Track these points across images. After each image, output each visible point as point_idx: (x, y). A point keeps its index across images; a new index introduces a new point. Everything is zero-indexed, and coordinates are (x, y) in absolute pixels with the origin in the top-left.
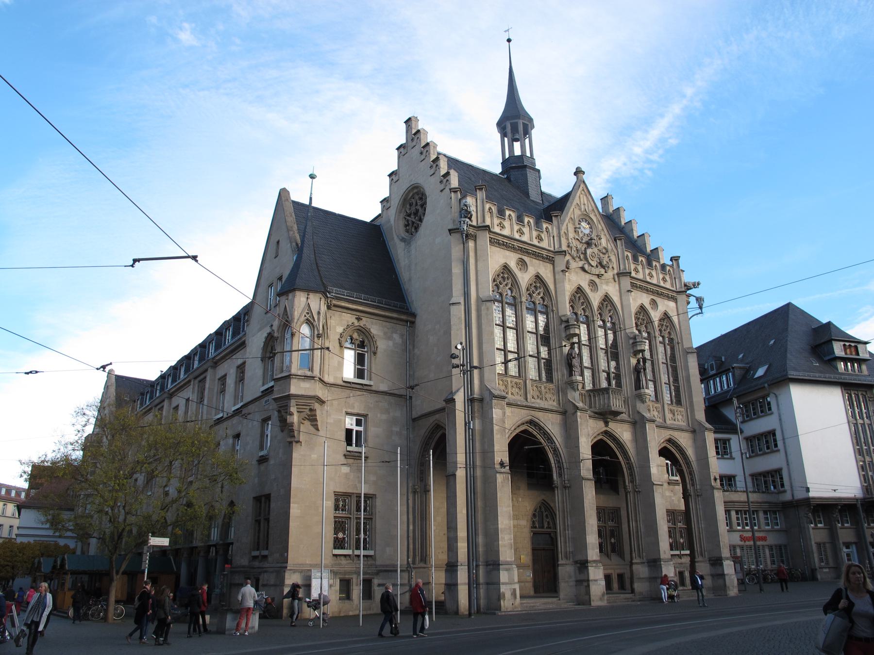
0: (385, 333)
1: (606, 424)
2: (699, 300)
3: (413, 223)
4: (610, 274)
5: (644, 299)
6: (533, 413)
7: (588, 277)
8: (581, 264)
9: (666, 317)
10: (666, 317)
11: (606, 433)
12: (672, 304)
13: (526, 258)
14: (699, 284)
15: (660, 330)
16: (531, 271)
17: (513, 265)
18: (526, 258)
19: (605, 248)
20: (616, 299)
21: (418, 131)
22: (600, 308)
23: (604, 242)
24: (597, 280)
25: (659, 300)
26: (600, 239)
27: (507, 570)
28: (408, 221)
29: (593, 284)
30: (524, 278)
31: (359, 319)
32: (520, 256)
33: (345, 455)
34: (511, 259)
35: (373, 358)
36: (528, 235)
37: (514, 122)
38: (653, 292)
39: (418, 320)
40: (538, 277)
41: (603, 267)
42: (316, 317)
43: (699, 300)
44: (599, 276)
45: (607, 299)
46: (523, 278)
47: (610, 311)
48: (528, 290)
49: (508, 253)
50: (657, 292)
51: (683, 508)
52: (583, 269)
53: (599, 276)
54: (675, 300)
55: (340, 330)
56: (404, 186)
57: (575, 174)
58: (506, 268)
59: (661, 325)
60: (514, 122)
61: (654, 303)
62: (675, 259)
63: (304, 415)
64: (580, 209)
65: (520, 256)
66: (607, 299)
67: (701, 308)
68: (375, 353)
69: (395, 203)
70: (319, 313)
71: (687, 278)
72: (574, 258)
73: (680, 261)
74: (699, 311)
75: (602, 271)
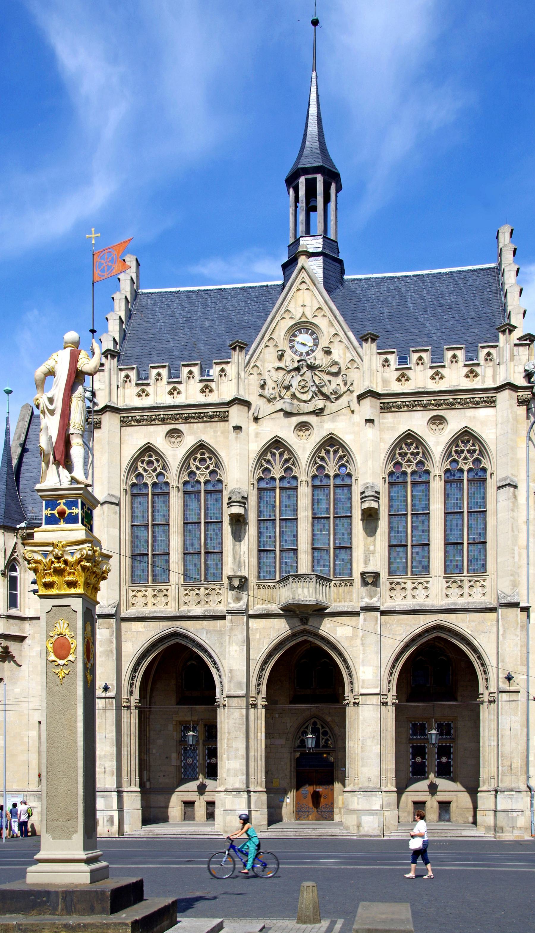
1: (304, 621)
4: (343, 401)
6: (177, 623)
7: (295, 420)
8: (279, 405)
12: (484, 413)
16: (189, 441)
19: (337, 364)
23: (338, 353)
24: (312, 419)
27: (103, 797)
32: (172, 427)
36: (191, 393)
38: (438, 405)
40: (201, 447)
44: (319, 412)
46: (175, 455)
49: (152, 428)
54: (492, 403)
58: (148, 450)
72: (269, 400)
75: (320, 403)
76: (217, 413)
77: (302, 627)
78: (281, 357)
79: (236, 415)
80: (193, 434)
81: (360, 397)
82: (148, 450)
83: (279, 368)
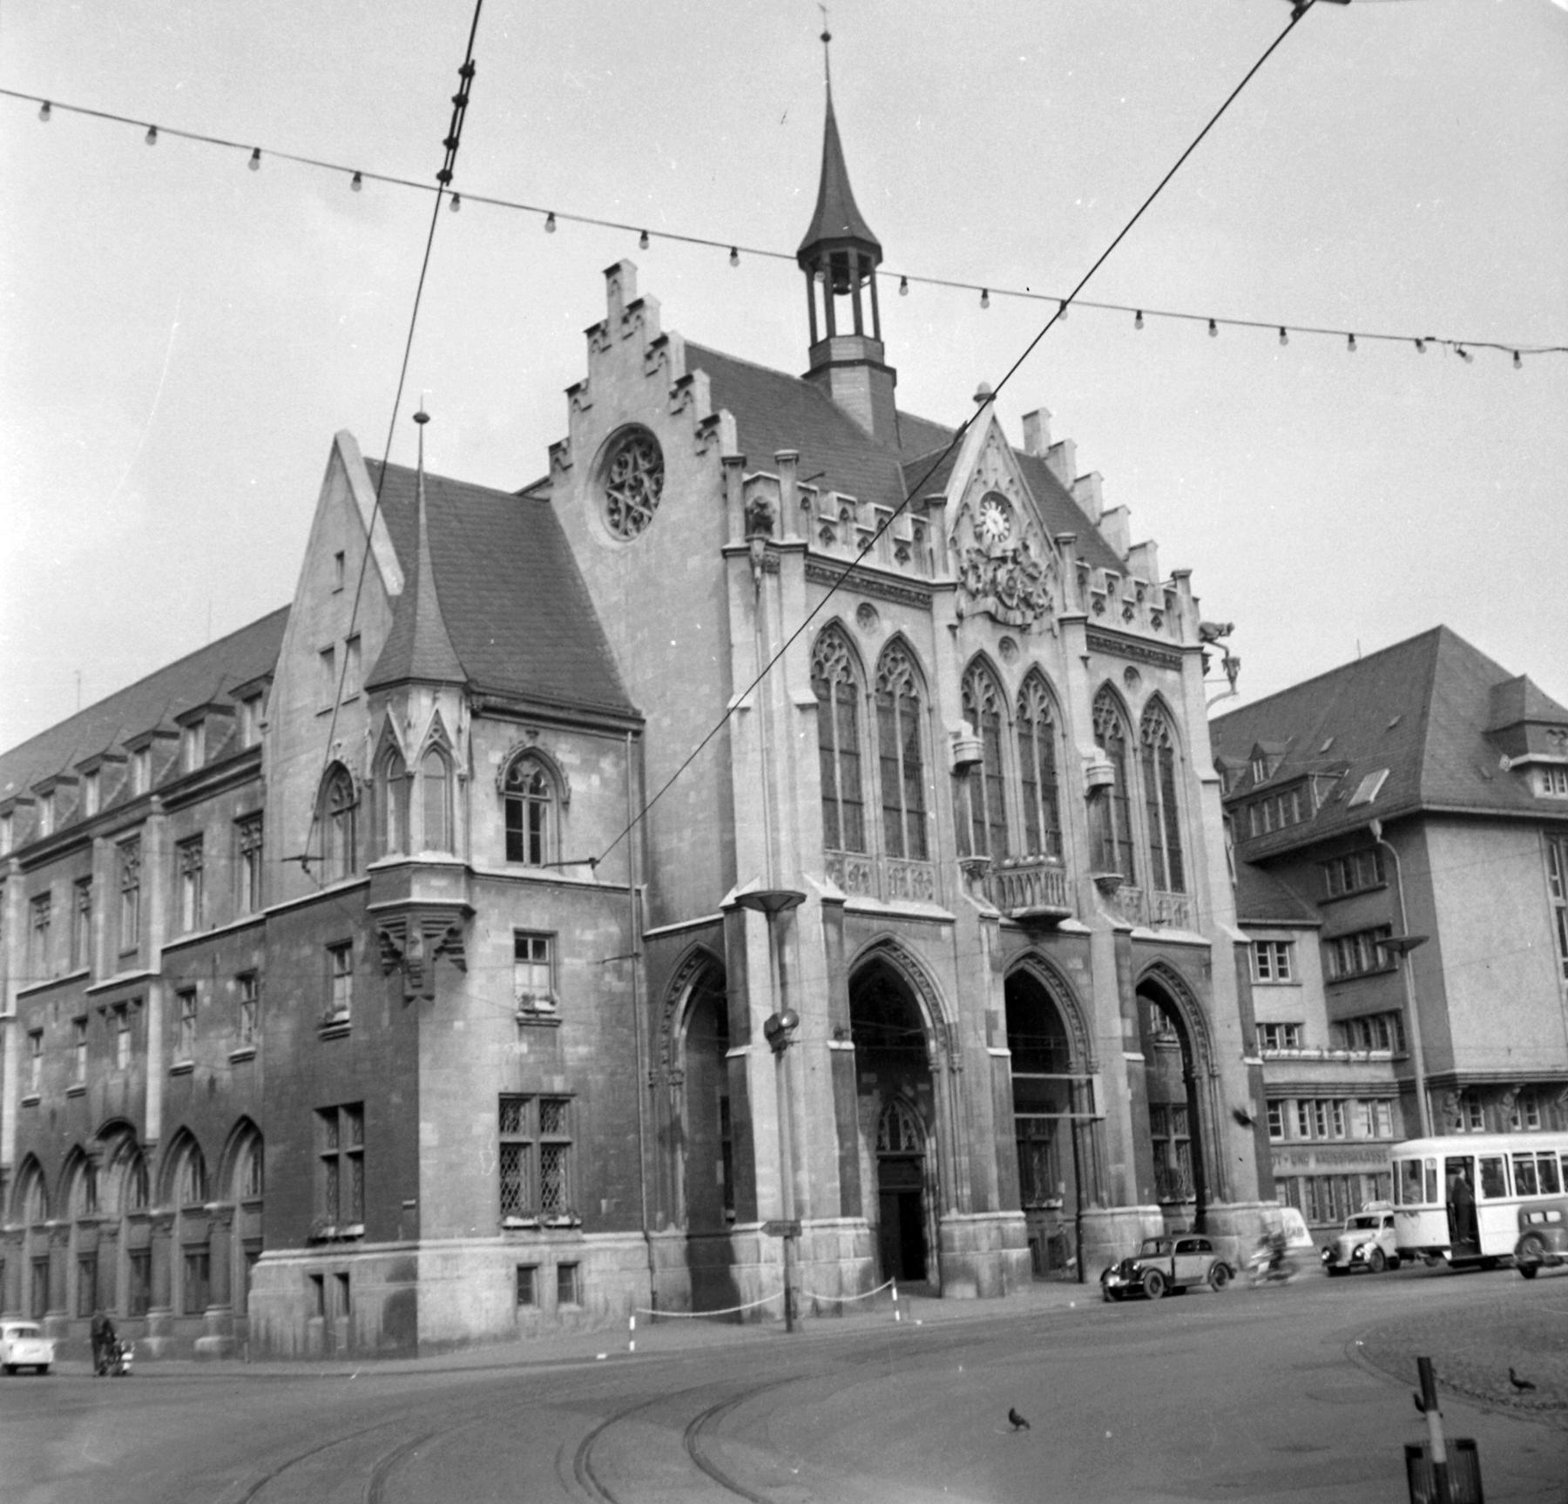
0: (584, 761)
2: (1231, 664)
3: (629, 508)
5: (1112, 669)
9: (1156, 702)
10: (1156, 702)
11: (1031, 955)
12: (1171, 675)
13: (877, 604)
14: (1230, 628)
15: (1145, 733)
17: (850, 619)
18: (877, 604)
19: (1035, 565)
20: (1053, 674)
21: (638, 304)
22: (1021, 694)
24: (1014, 635)
25: (1143, 669)
26: (1026, 547)
28: (616, 501)
29: (1006, 644)
30: (871, 646)
31: (533, 734)
33: (521, 1023)
34: (844, 606)
35: (562, 814)
37: (838, 255)
39: (649, 729)
40: (898, 642)
41: (1030, 606)
42: (452, 737)
43: (1231, 664)
45: (1035, 675)
47: (1042, 698)
48: (879, 668)
50: (1138, 653)
51: (1185, 1099)
52: (992, 617)
53: (1024, 629)
54: (1178, 667)
55: (496, 758)
56: (606, 423)
57: (977, 398)
58: (834, 627)
59: (1146, 721)
60: (838, 255)
61: (1131, 674)
62: (1181, 576)
63: (437, 942)
64: (985, 483)
65: (862, 599)
66: (1035, 675)
67: (1232, 679)
68: (566, 804)
69: (584, 457)
70: (459, 731)
71: (1210, 614)
72: (973, 595)
73: (1192, 578)
74: (1227, 686)
75: (1030, 614)
76: (919, 597)
77: (1029, 949)
78: (979, 537)
79: (945, 608)
80: (893, 619)
81: (1062, 621)
82: (834, 627)
83: (979, 551)
